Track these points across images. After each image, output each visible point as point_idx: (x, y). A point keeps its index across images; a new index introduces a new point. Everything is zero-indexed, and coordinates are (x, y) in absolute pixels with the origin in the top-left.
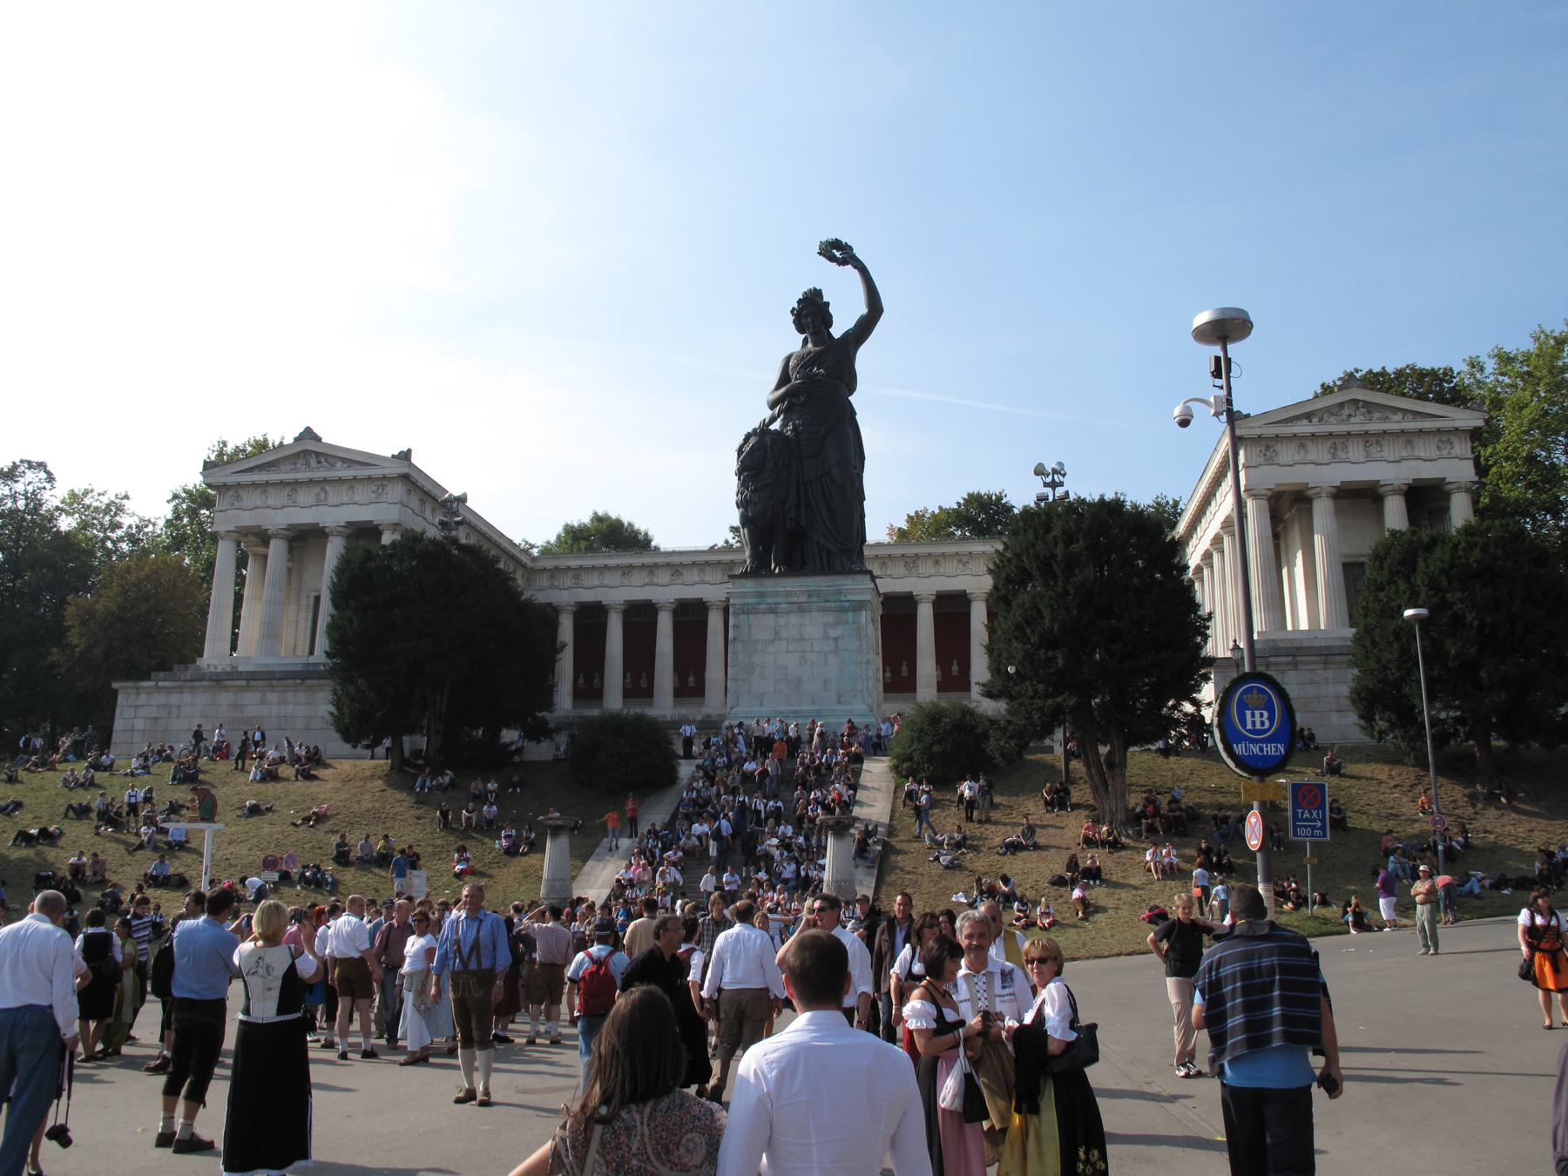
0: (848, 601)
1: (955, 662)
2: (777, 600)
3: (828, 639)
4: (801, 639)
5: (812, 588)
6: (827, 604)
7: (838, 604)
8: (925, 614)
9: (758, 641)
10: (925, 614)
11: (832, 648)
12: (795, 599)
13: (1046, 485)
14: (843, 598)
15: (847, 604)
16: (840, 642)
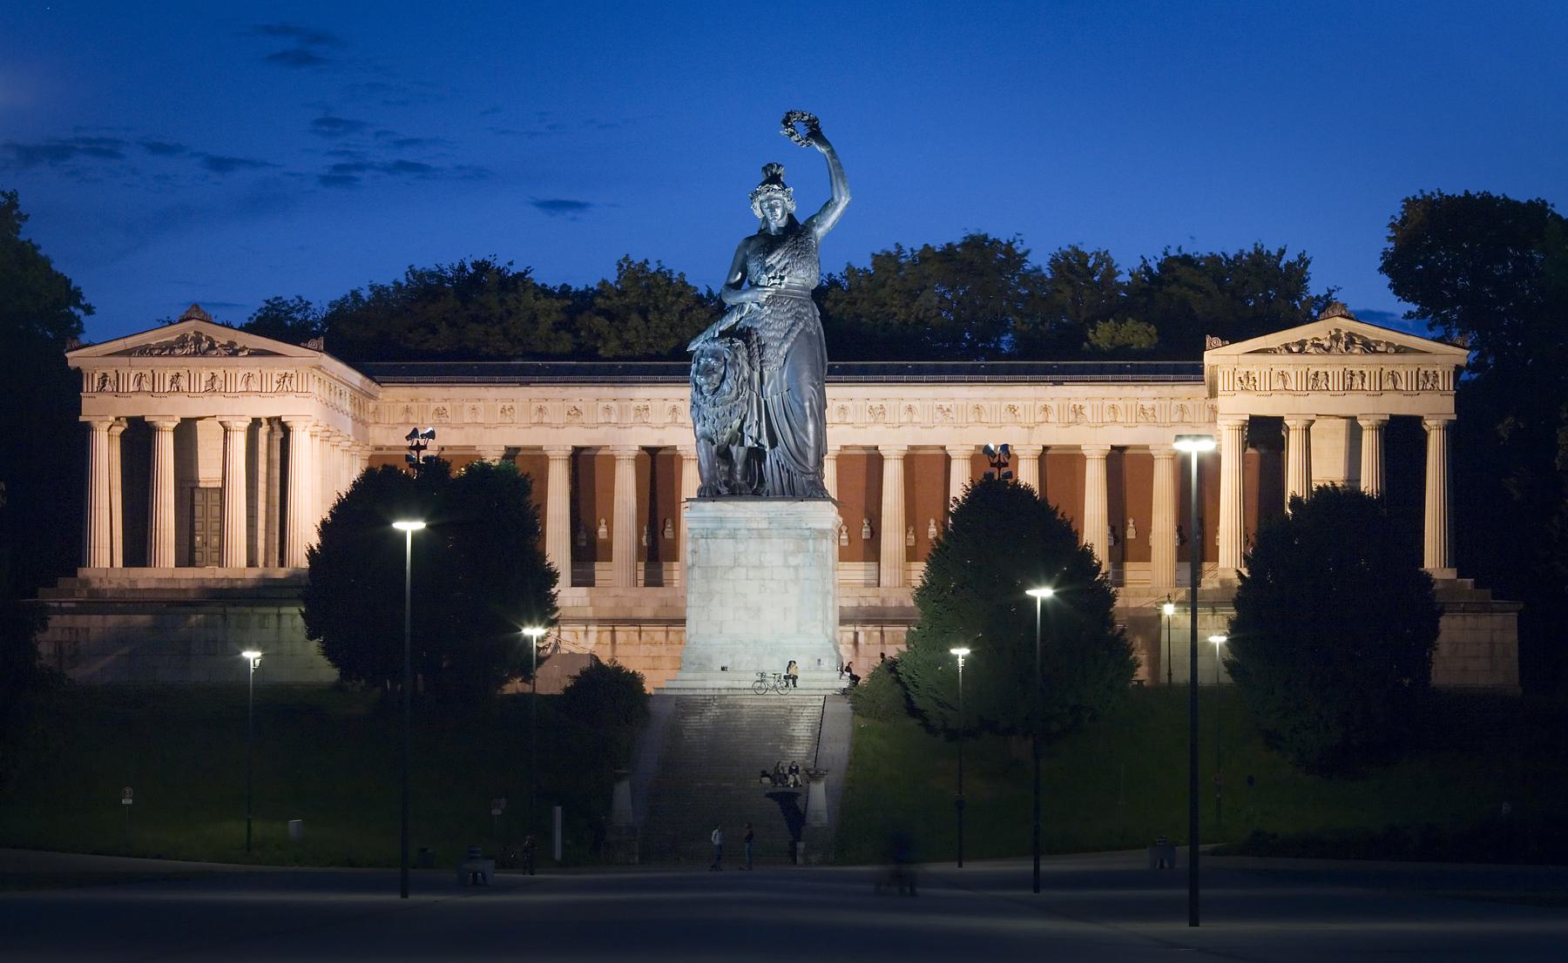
0: (810, 529)
1: (932, 522)
2: (738, 526)
3: (789, 567)
4: (761, 566)
5: (772, 515)
7: (799, 531)
8: (893, 476)
9: (717, 567)
10: (893, 476)
12: (754, 525)
13: (993, 465)
14: (804, 526)
15: (807, 533)
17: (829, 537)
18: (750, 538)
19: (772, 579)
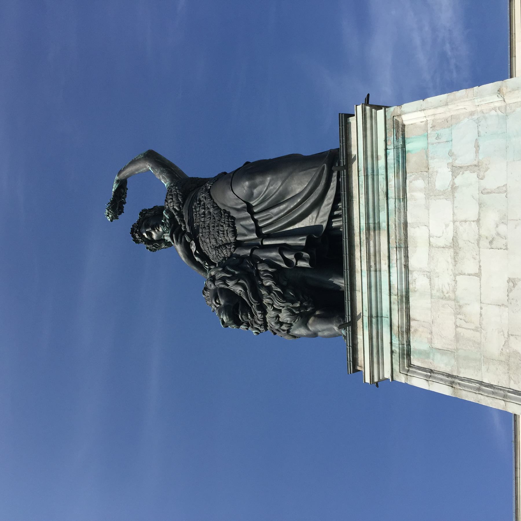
3: (454, 188)
6: (391, 194)
9: (457, 338)
11: (471, 177)
14: (381, 163)
16: (458, 163)
17: (399, 113)
18: (406, 267)
19: (478, 221)
